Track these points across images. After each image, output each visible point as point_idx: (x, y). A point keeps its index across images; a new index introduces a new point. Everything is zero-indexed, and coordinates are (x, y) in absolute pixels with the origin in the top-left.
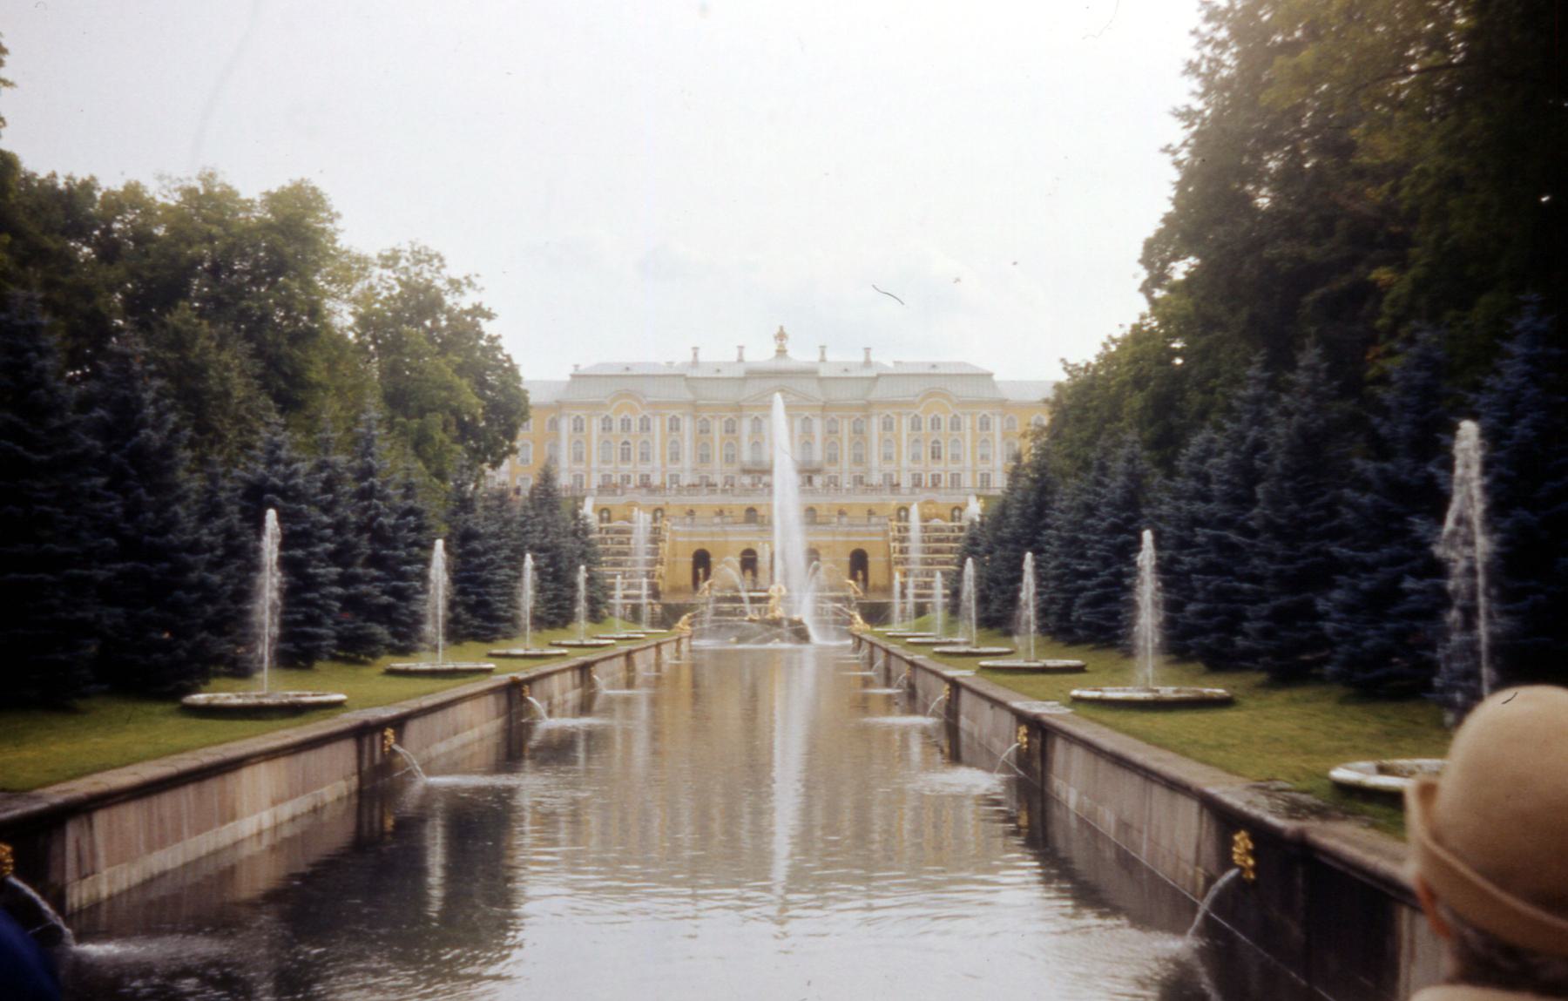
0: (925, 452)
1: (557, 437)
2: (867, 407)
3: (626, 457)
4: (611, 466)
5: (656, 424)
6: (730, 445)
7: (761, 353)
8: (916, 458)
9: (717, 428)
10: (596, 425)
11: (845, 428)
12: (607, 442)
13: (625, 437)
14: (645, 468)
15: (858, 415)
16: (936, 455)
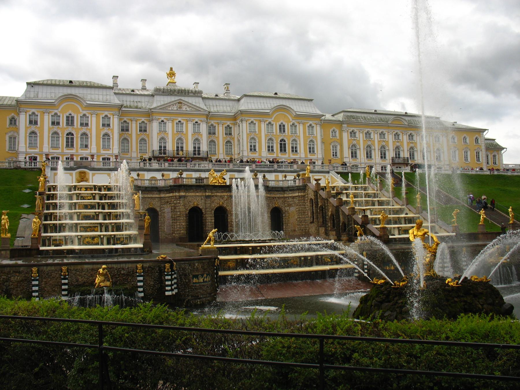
0: (276, 147)
1: (17, 130)
2: (236, 117)
3: (70, 143)
4: (60, 151)
5: (93, 122)
6: (143, 140)
7: (163, 82)
8: (270, 149)
9: (134, 128)
10: (47, 120)
11: (220, 131)
12: (56, 133)
13: (70, 129)
14: (85, 153)
15: (228, 123)
16: (283, 148)
